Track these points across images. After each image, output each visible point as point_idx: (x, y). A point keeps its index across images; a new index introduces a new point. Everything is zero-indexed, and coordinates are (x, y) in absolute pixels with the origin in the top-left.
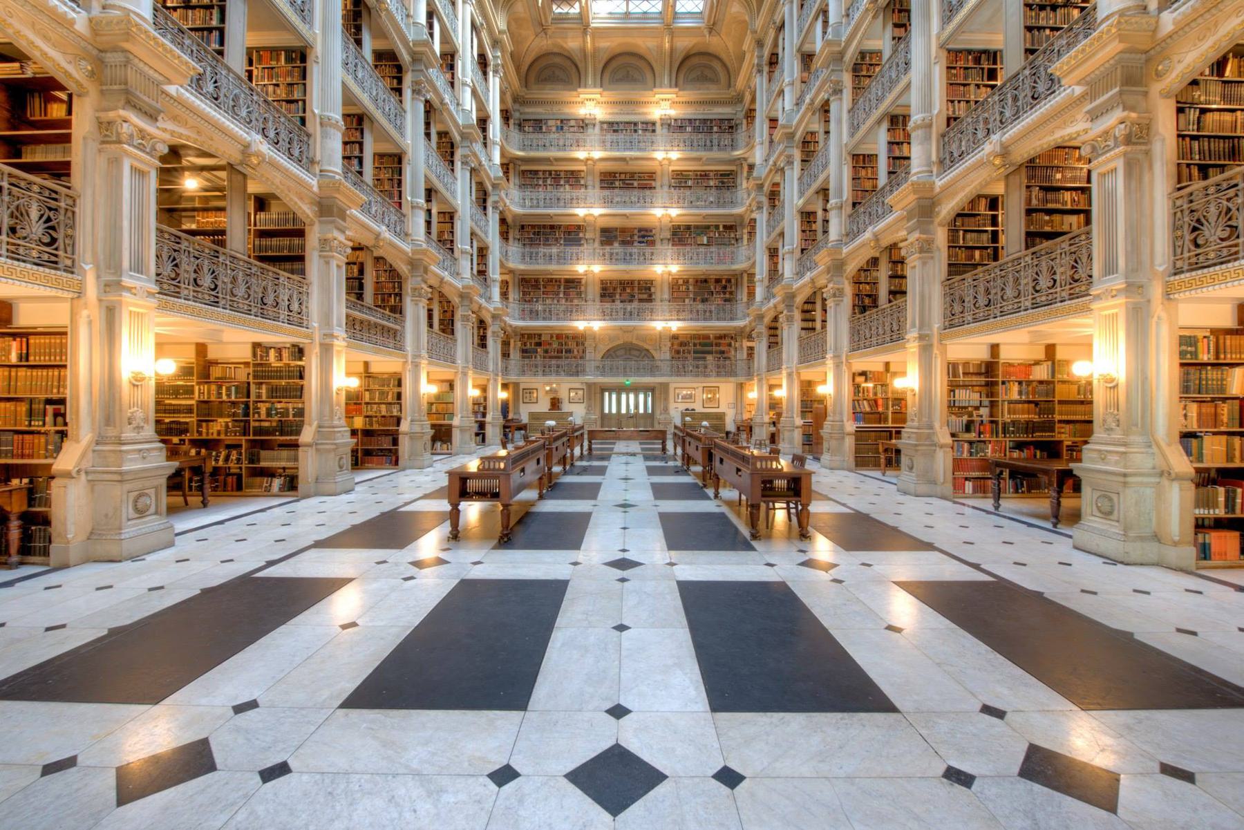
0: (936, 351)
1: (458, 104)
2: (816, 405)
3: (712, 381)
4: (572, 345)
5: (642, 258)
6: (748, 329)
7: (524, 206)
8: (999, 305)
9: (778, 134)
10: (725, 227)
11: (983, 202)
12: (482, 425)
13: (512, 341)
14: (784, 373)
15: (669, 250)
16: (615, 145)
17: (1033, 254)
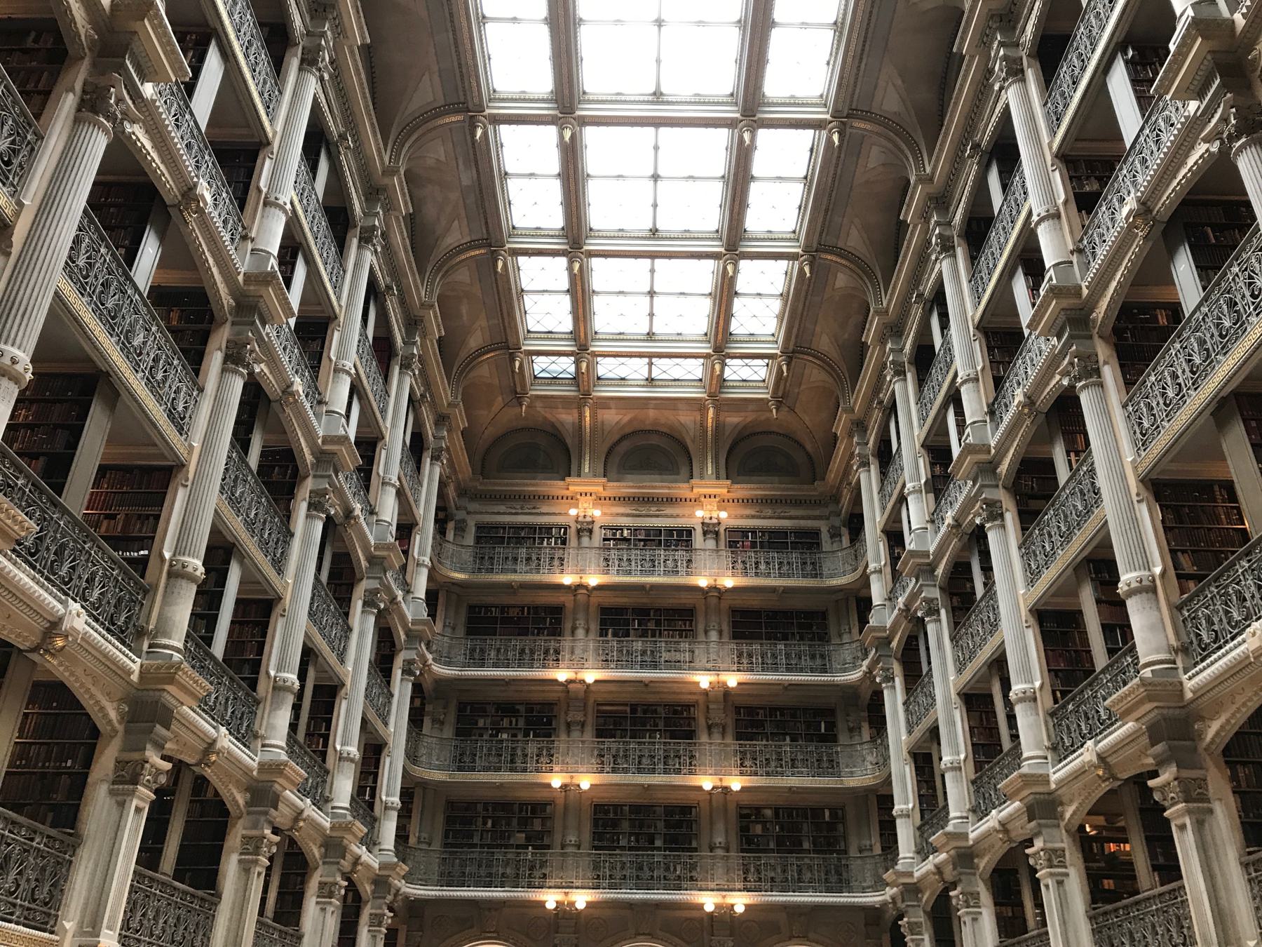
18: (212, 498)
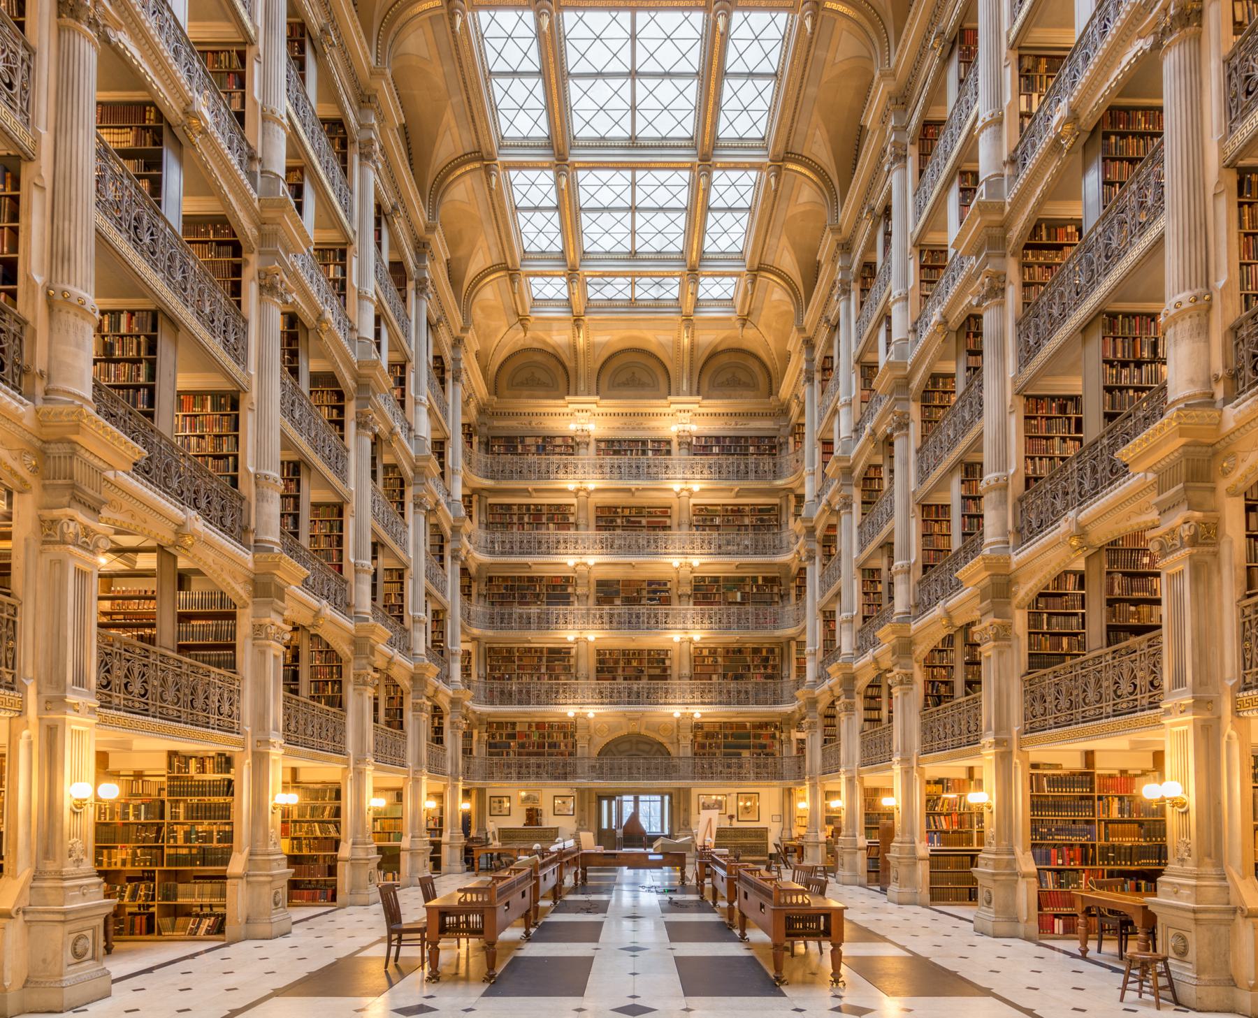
0: (1015, 760)
1: (410, 429)
2: (884, 821)
3: (749, 787)
4: (558, 737)
5: (652, 621)
6: (797, 716)
7: (492, 552)
8: (1081, 709)
9: (832, 468)
10: (764, 578)
11: (1072, 580)
12: (437, 847)
13: (475, 732)
14: (843, 778)
15: (690, 609)
16: (617, 471)
17: (1114, 652)
18: (276, 418)
